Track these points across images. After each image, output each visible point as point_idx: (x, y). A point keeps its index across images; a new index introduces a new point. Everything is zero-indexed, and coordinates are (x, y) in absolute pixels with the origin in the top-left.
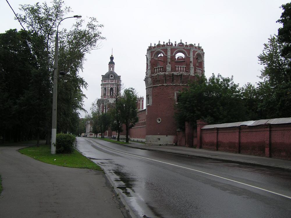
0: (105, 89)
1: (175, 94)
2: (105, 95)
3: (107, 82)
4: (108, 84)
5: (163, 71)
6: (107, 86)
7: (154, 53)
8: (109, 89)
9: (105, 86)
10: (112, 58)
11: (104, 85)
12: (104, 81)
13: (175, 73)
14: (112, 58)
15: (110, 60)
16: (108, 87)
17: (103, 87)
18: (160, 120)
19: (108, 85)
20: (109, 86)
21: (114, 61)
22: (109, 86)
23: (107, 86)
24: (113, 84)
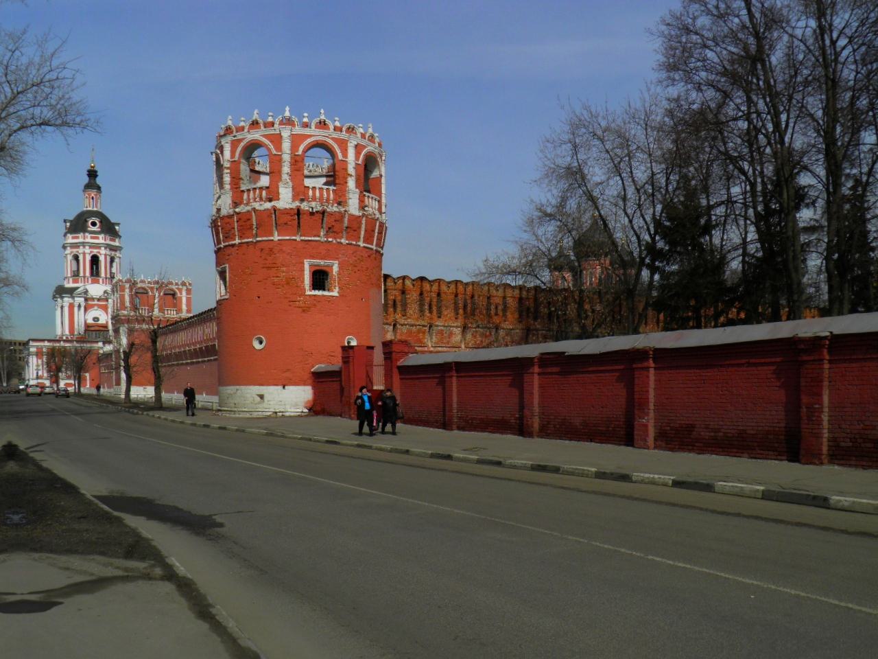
0: (76, 258)
1: (307, 267)
2: (76, 274)
3: (81, 240)
4: (84, 244)
5: (270, 200)
7: (242, 144)
8: (88, 258)
10: (92, 174)
13: (305, 206)
14: (92, 174)
15: (86, 180)
16: (84, 254)
18: (261, 343)
19: (84, 247)
21: (99, 181)
22: (87, 250)
24: (98, 246)
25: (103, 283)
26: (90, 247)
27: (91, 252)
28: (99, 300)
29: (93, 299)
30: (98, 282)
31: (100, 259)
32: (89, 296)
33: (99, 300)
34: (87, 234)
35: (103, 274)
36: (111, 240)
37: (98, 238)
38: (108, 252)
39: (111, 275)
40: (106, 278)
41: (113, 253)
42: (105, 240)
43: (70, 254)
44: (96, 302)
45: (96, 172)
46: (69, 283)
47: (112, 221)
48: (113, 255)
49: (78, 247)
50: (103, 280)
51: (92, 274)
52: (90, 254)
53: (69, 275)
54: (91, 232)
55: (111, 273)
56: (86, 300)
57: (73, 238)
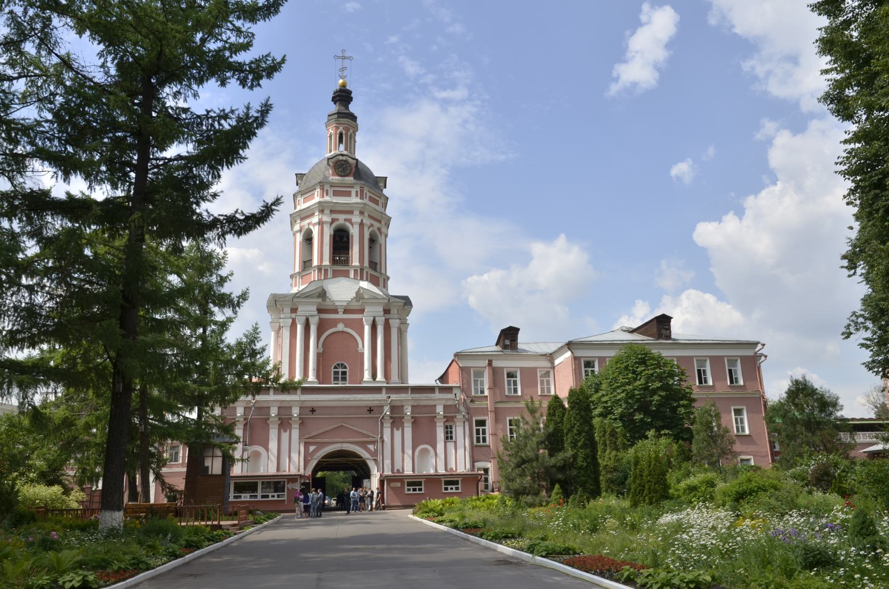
2: (306, 264)
3: (317, 199)
4: (321, 208)
6: (315, 219)
8: (328, 232)
10: (343, 97)
11: (302, 219)
12: (300, 199)
14: (343, 97)
15: (334, 108)
17: (297, 227)
20: (327, 218)
21: (353, 108)
22: (327, 218)
23: (315, 219)
26: (332, 212)
27: (333, 221)
30: (346, 274)
32: (327, 305)
33: (346, 311)
35: (356, 262)
36: (371, 199)
37: (348, 194)
38: (367, 221)
40: (362, 270)
41: (376, 224)
42: (362, 198)
43: (300, 231)
44: (341, 316)
45: (350, 92)
46: (295, 286)
47: (376, 174)
48: (375, 229)
49: (312, 215)
50: (356, 271)
51: (334, 262)
52: (331, 224)
53: (297, 270)
56: (320, 311)
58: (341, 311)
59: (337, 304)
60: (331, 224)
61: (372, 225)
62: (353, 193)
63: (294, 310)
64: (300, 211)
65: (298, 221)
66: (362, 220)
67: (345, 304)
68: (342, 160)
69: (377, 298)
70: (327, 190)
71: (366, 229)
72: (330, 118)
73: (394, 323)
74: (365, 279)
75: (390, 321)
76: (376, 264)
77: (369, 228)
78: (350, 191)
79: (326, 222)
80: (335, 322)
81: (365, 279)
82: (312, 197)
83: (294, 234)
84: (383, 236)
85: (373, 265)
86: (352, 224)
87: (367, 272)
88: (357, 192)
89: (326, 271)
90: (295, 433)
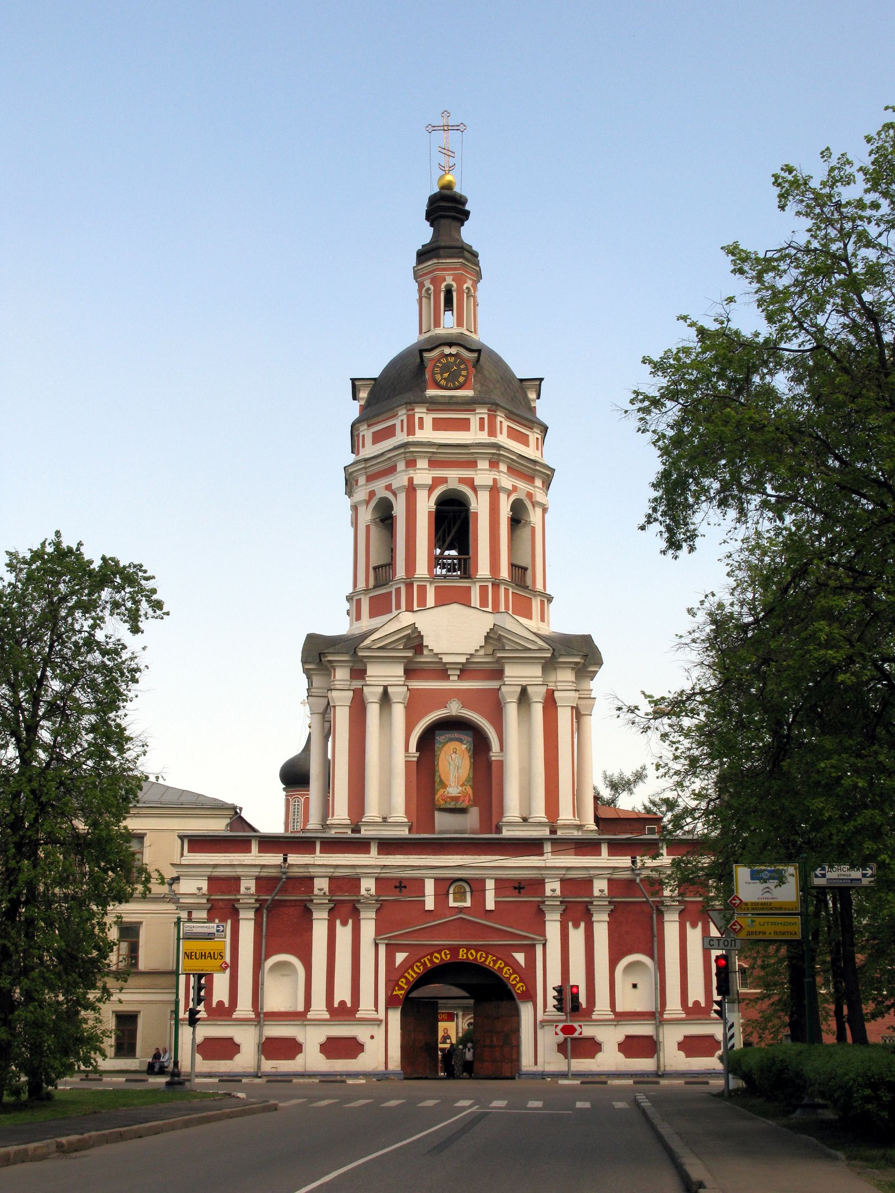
3: (401, 437)
8: (426, 505)
9: (379, 486)
11: (370, 478)
12: (367, 433)
16: (411, 489)
17: (361, 494)
19: (411, 464)
21: (468, 233)
22: (423, 475)
23: (399, 480)
25: (484, 602)
26: (434, 464)
27: (437, 481)
28: (465, 671)
29: (442, 671)
31: (473, 506)
34: (420, 412)
35: (483, 569)
36: (513, 434)
37: (464, 425)
38: (506, 482)
39: (511, 574)
40: (496, 586)
41: (522, 485)
42: (492, 433)
43: (367, 503)
44: (454, 684)
48: (523, 496)
49: (392, 470)
50: (483, 590)
52: (431, 489)
53: (361, 585)
54: (434, 404)
55: (513, 566)
56: (410, 673)
57: (378, 437)
58: (454, 674)
59: (446, 659)
60: (431, 489)
61: (515, 488)
62: (474, 421)
63: (359, 673)
64: (366, 460)
65: (362, 480)
66: (495, 480)
67: (463, 659)
68: (450, 355)
69: (530, 649)
70: (421, 419)
71: (503, 497)
72: (423, 258)
73: (565, 699)
74: (502, 609)
75: (557, 694)
76: (526, 569)
77: (509, 496)
78: (469, 419)
79: (423, 486)
80: (442, 698)
81: (502, 609)
82: (389, 432)
83: (355, 508)
84: (539, 511)
85: (520, 573)
86: (475, 489)
87: (506, 590)
88: (482, 419)
89: (422, 590)
90: (368, 928)
